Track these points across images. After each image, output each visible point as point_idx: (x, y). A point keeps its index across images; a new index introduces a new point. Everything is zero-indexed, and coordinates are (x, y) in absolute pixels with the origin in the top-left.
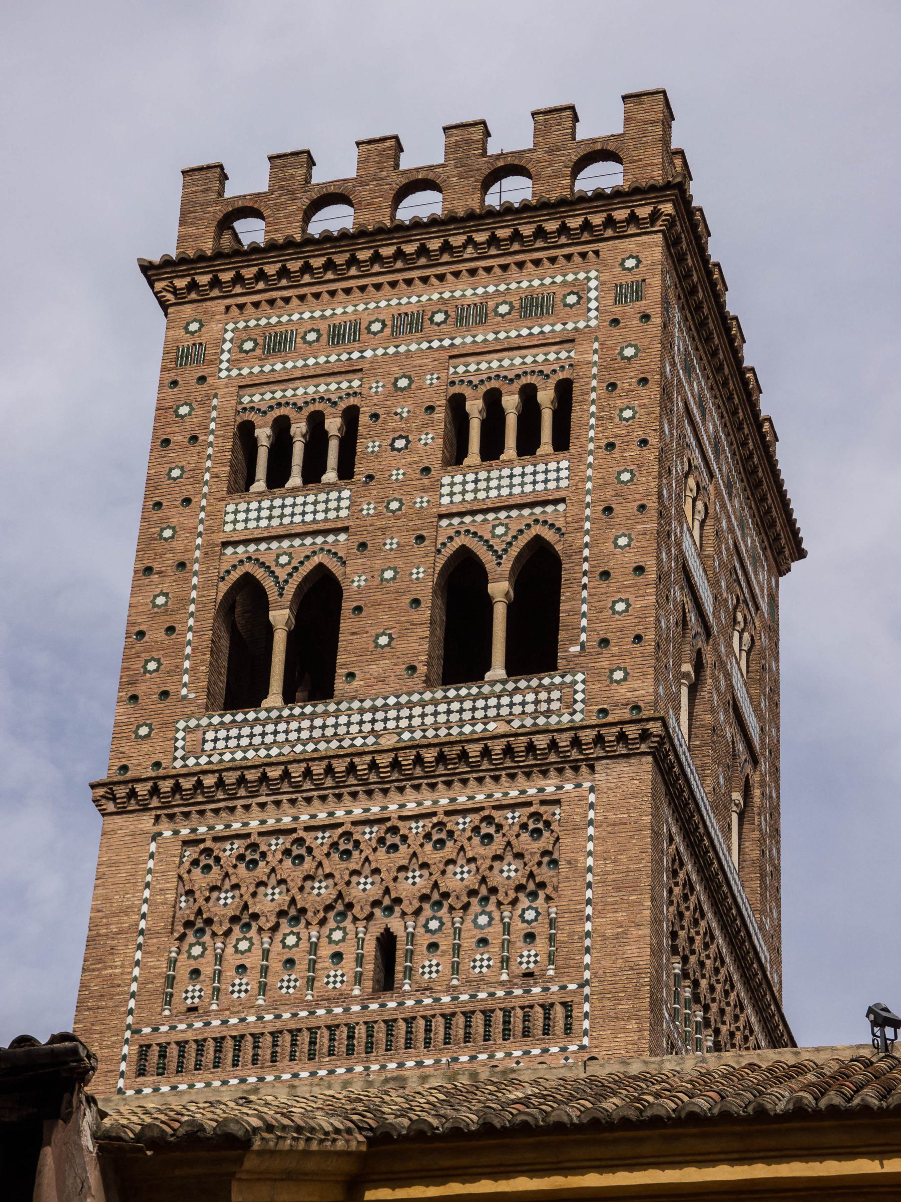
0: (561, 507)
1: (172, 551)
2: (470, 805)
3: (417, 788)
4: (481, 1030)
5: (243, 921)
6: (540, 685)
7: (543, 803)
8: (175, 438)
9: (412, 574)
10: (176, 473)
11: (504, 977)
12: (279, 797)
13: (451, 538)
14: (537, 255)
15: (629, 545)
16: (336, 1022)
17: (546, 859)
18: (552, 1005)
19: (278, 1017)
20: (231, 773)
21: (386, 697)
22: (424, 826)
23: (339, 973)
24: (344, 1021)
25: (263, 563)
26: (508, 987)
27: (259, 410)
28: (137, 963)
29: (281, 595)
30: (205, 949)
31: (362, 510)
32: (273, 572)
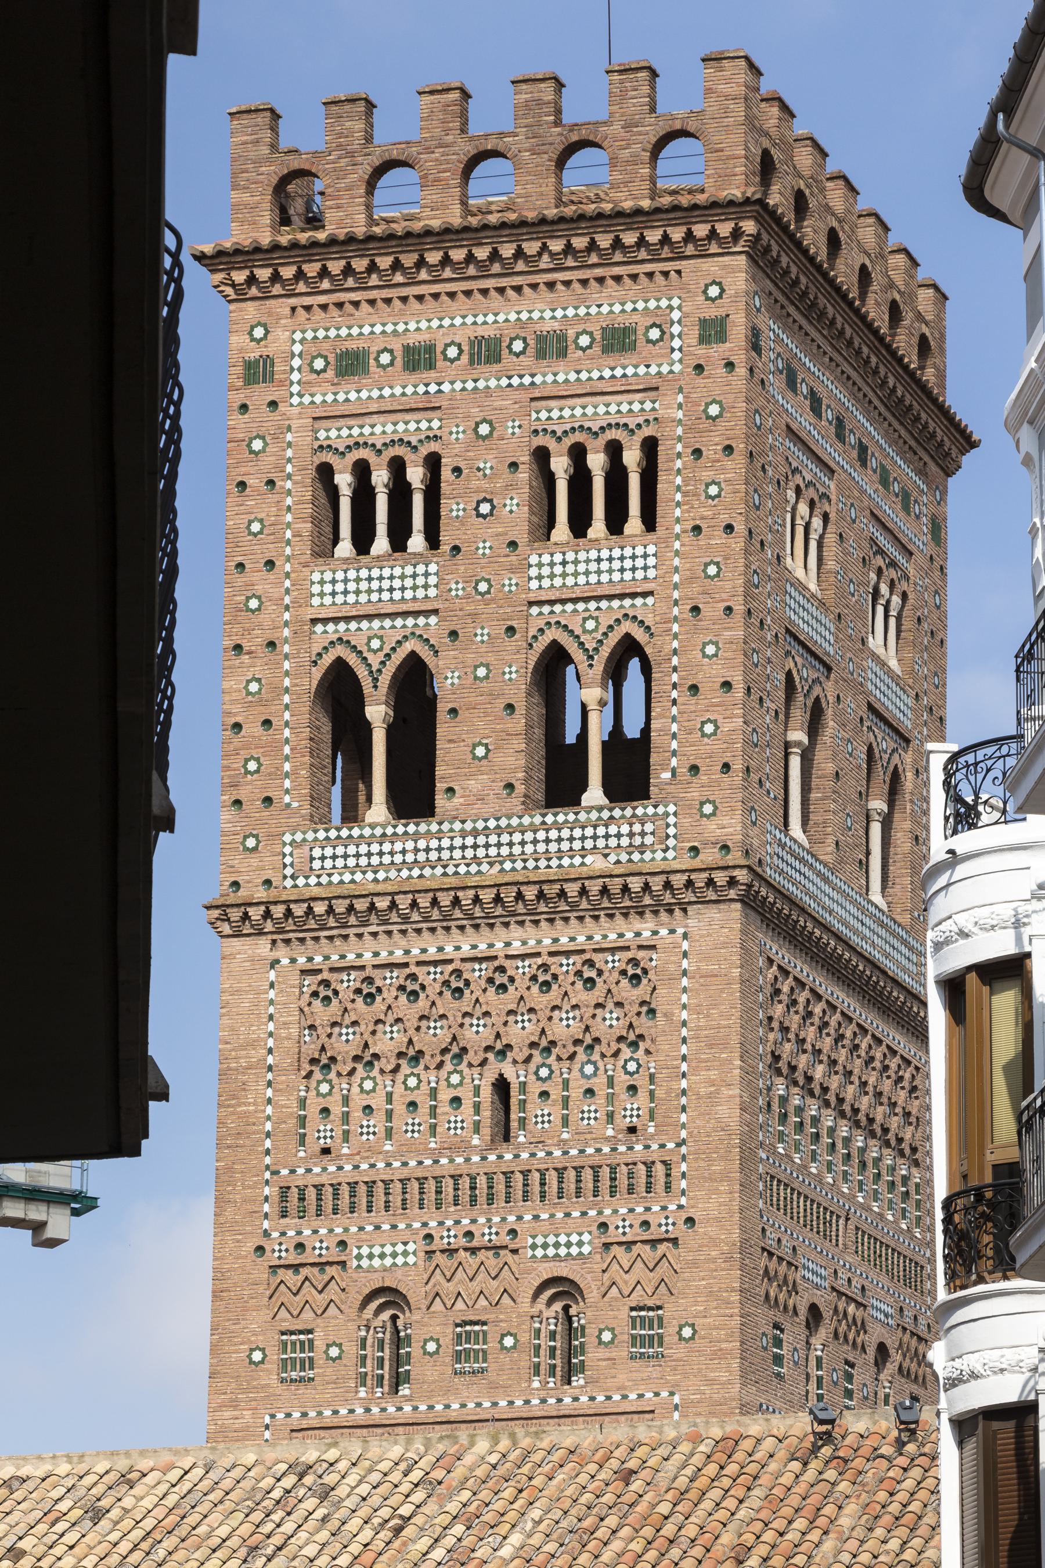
0: (650, 600)
1: (260, 626)
2: (572, 947)
3: (521, 923)
4: (591, 1185)
5: (366, 1059)
6: (634, 816)
7: (640, 947)
8: (251, 481)
9: (504, 673)
10: (256, 527)
11: (610, 1132)
12: (390, 928)
13: (541, 630)
14: (617, 270)
15: (716, 655)
16: (458, 1172)
17: (644, 1009)
18: (653, 1163)
19: (405, 1164)
20: (340, 901)
21: (486, 813)
22: (530, 966)
23: (459, 1119)
24: (465, 1172)
25: (355, 647)
26: (613, 1142)
27: (336, 449)
28: (269, 1101)
29: (375, 687)
30: (332, 1087)
31: (450, 590)
32: (365, 659)
